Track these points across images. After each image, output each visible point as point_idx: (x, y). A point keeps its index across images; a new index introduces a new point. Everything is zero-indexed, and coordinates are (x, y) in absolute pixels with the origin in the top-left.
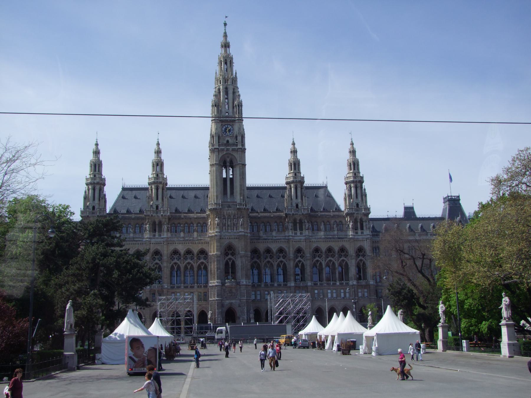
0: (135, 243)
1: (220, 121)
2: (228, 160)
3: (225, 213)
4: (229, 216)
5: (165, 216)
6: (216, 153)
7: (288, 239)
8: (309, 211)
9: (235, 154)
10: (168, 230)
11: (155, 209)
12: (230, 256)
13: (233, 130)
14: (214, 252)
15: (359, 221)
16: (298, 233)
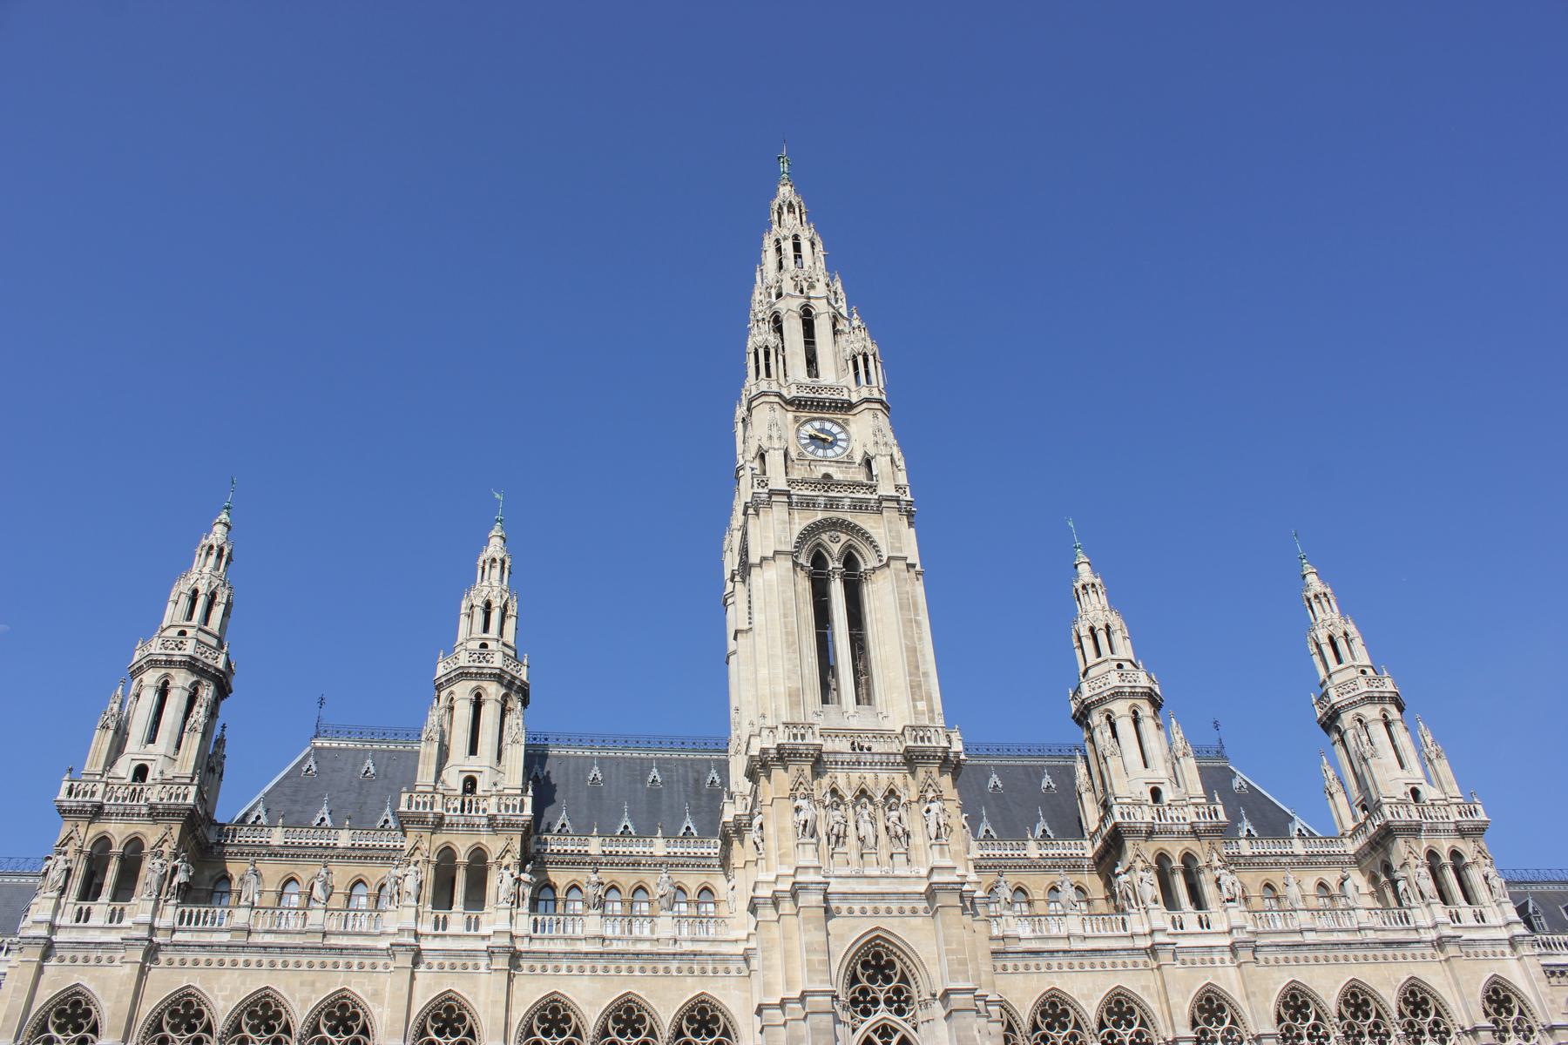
0: (330, 960)
1: (790, 402)
2: (836, 549)
3: (841, 782)
4: (863, 792)
5: (509, 825)
6: (779, 511)
7: (1153, 951)
8: (1222, 817)
9: (864, 521)
10: (516, 900)
11: (460, 791)
12: (882, 1014)
13: (848, 440)
14: (789, 984)
15: (1445, 859)
16: (1189, 916)
